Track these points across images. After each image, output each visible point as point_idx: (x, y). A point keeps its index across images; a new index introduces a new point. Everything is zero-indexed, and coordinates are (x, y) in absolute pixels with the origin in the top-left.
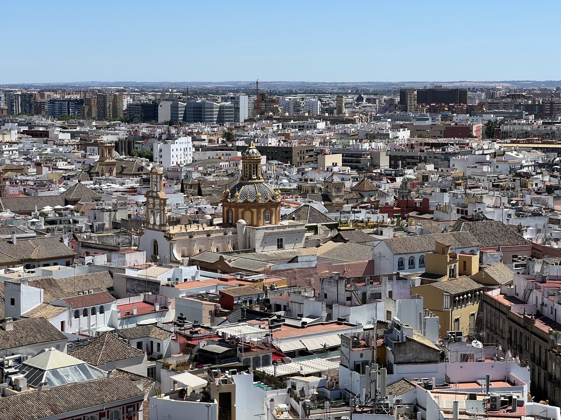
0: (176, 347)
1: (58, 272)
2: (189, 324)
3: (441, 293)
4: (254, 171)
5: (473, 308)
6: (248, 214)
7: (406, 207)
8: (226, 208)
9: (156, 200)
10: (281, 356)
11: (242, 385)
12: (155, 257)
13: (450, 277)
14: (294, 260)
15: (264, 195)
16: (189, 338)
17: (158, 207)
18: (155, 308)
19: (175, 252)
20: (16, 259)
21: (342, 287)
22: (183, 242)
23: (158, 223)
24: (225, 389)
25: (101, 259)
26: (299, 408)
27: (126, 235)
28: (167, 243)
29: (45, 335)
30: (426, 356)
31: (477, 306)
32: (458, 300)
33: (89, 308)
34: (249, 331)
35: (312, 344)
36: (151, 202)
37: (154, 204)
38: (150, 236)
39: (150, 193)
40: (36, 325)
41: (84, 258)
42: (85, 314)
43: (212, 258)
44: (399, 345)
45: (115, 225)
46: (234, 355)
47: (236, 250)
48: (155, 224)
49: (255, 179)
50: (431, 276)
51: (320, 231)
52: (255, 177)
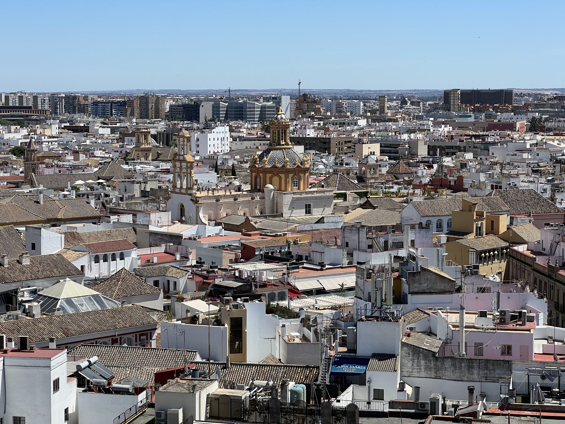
0: (192, 285)
1: (81, 228)
2: (205, 267)
3: (467, 249)
4: (282, 136)
5: (500, 265)
6: (276, 179)
7: (438, 184)
8: (254, 174)
9: (183, 164)
10: (295, 293)
11: (253, 312)
12: (181, 216)
13: (477, 235)
14: (321, 221)
15: (293, 160)
16: (206, 278)
17: (185, 171)
18: (176, 257)
19: (201, 215)
20: (42, 218)
21: (363, 234)
22: (209, 206)
23: (185, 187)
24: (236, 314)
25: (127, 219)
26: (310, 335)
27: (154, 202)
28: (194, 206)
29: (60, 269)
30: (440, 286)
31: (504, 264)
32: (485, 256)
33: (110, 254)
34: (266, 271)
35: (330, 283)
36: (178, 166)
37: (181, 168)
38: (177, 200)
39: (177, 157)
40: (53, 261)
41: (110, 217)
42: (105, 260)
43: (239, 220)
44: (414, 274)
45: (144, 194)
46: (248, 289)
47: (263, 214)
48: (181, 187)
49: (283, 145)
50: (456, 233)
51: (349, 198)
52: (284, 143)
